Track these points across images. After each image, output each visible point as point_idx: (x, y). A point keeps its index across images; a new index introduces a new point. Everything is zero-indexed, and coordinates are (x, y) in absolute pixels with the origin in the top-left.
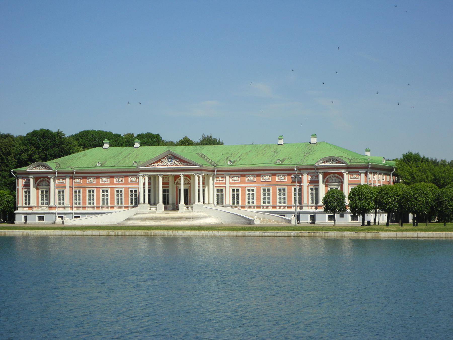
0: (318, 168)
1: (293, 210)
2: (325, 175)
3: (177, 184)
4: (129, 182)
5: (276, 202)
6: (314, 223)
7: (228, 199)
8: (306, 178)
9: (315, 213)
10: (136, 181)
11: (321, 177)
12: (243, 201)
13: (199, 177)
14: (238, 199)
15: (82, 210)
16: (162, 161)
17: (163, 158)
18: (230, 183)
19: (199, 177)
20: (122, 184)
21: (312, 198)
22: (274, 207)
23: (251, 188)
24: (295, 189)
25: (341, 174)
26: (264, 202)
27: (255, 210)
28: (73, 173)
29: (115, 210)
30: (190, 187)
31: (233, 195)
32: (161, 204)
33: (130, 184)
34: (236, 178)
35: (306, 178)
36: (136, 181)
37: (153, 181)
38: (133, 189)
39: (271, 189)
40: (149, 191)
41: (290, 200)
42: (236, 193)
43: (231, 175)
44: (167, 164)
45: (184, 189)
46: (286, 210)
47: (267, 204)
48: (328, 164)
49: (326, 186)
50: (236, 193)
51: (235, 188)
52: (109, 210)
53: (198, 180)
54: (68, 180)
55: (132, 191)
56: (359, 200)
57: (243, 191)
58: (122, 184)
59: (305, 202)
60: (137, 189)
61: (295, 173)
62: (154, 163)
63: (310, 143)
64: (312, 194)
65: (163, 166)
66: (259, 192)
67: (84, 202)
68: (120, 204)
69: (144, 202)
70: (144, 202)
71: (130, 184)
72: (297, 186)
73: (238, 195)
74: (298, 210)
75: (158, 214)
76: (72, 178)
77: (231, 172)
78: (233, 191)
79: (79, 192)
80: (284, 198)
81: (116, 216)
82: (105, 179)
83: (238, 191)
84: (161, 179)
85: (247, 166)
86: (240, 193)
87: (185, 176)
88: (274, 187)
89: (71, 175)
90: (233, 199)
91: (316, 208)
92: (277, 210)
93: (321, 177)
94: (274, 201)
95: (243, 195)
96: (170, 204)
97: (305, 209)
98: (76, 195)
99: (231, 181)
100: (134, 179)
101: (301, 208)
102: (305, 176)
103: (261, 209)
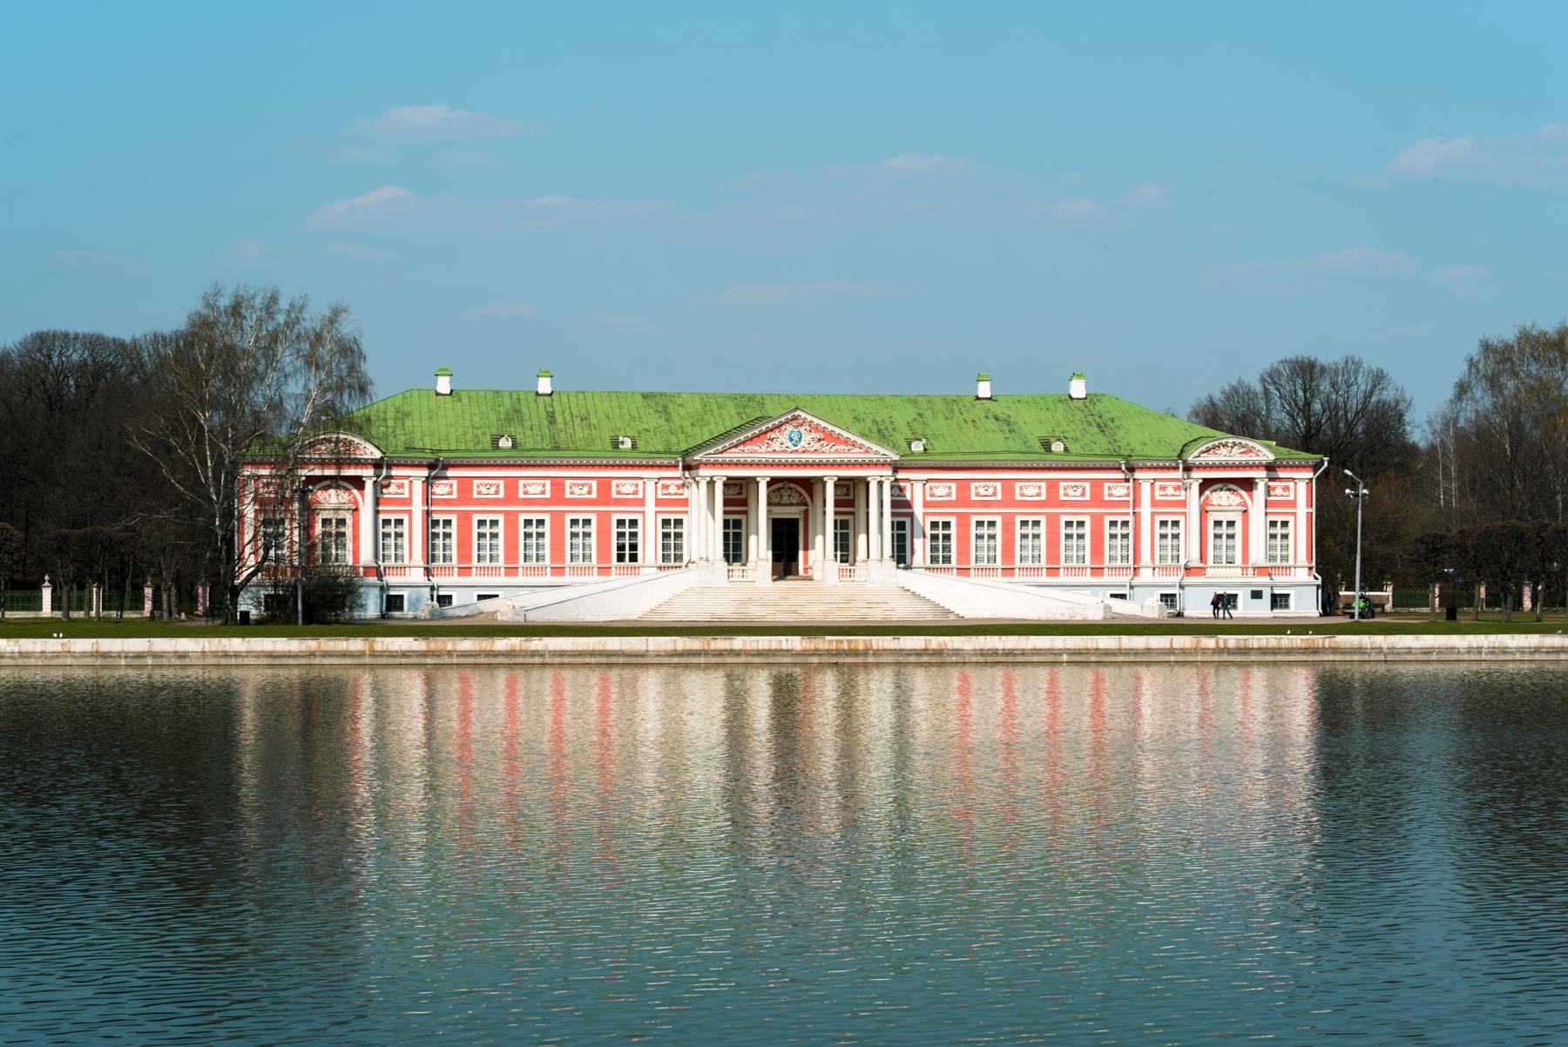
5: (1058, 558)
10: (636, 493)
12: (964, 554)
13: (880, 484)
14: (947, 548)
19: (880, 484)
30: (806, 513)
36: (636, 493)
38: (627, 517)
39: (953, 521)
48: (1222, 456)
49: (1203, 513)
51: (941, 519)
60: (639, 517)
62: (743, 443)
63: (978, 398)
73: (947, 537)
85: (953, 458)
86: (953, 531)
89: (425, 473)
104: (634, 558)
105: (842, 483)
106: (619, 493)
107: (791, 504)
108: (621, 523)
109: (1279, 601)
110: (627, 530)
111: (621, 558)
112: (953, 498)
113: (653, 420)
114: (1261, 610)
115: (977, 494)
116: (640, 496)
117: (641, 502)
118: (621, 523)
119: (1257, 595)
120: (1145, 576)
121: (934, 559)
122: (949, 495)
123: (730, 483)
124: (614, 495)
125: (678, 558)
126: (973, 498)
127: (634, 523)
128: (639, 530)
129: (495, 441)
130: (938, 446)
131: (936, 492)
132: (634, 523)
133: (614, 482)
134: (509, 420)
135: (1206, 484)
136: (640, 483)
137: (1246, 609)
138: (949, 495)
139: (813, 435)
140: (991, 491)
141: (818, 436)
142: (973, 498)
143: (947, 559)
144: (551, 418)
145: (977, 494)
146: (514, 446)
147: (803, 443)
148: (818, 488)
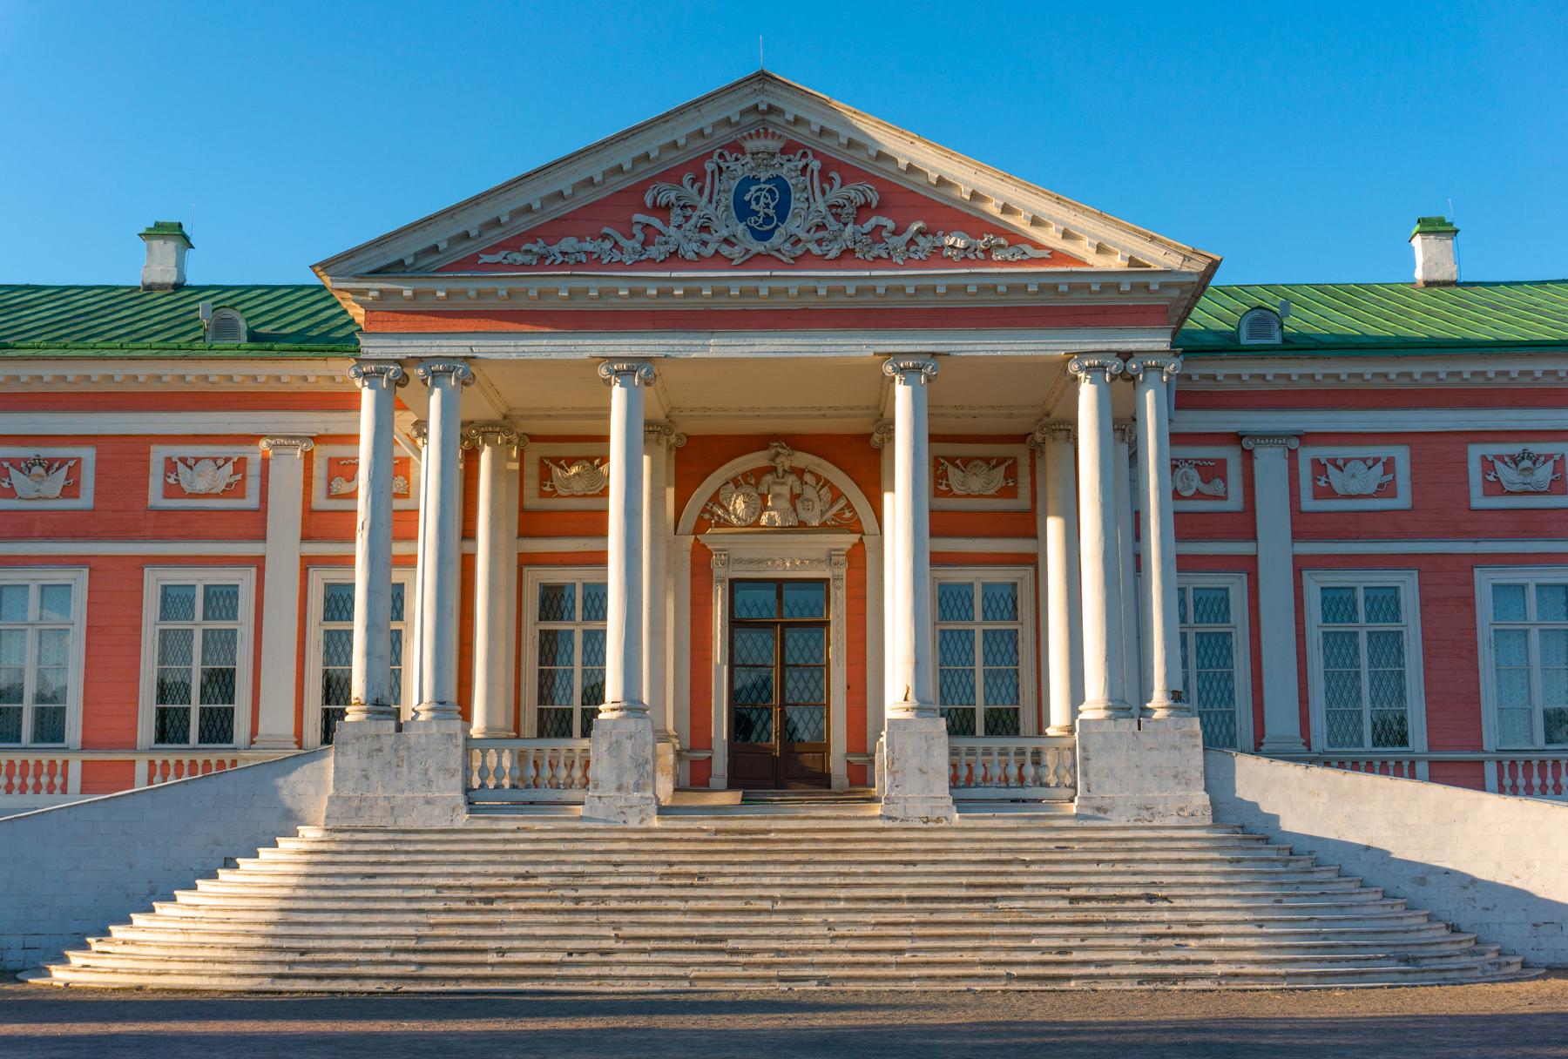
3: (700, 527)
4: (156, 498)
16: (662, 210)
17: (672, 176)
18: (1303, 526)
31: (1341, 646)
43: (1306, 438)
65: (674, 258)
78: (1337, 604)
99: (1308, 503)
104: (218, 728)
106: (173, 491)
107: (802, 527)
108: (174, 602)
110: (198, 625)
111: (169, 728)
112: (1403, 500)
115: (1494, 488)
116: (251, 501)
117: (254, 524)
118: (174, 602)
122: (1386, 490)
124: (155, 497)
126: (1478, 500)
127: (221, 601)
131: (1336, 478)
133: (158, 454)
136: (253, 454)
138: (1386, 490)
139: (837, 193)
140: (1544, 473)
141: (854, 192)
142: (1478, 500)
145: (1494, 488)
147: (793, 225)
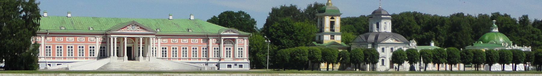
0: (221, 36)
1: (202, 61)
2: (224, 39)
6: (219, 69)
7: (160, 55)
8: (212, 41)
9: (219, 63)
11: (222, 40)
12: (170, 55)
14: (166, 54)
15: (51, 60)
18: (161, 44)
20: (83, 42)
21: (215, 54)
22: (190, 59)
23: (174, 47)
24: (203, 49)
25: (234, 40)
26: (183, 56)
27: (178, 61)
28: (46, 34)
29: (78, 60)
31: (163, 51)
32: (126, 57)
33: (89, 42)
34: (164, 40)
35: (212, 41)
37: (120, 41)
40: (117, 48)
41: (200, 55)
42: (164, 50)
44: (130, 30)
45: (127, 47)
46: (198, 61)
47: (185, 57)
48: (228, 33)
50: (164, 50)
51: (164, 47)
52: (73, 60)
53: (153, 41)
54: (43, 38)
55: (91, 47)
56: (303, 55)
57: (169, 49)
58: (83, 42)
59: (211, 57)
61: (206, 38)
64: (215, 52)
66: (180, 49)
67: (54, 54)
68: (81, 56)
69: (114, 55)
70: (114, 55)
71: (89, 42)
72: (205, 46)
73: (166, 51)
74: (205, 61)
75: (124, 63)
76: (46, 38)
77: (163, 36)
78: (163, 48)
79: (50, 47)
80: (196, 54)
81: (97, 64)
82: (71, 38)
83: (166, 48)
84: (126, 39)
86: (167, 50)
87: (128, 37)
88: (190, 47)
90: (163, 54)
91: (220, 60)
92: (192, 61)
93: (222, 40)
94: (190, 55)
95: (169, 51)
96: (131, 57)
97: (211, 61)
98: (47, 50)
100: (92, 39)
101: (208, 60)
102: (211, 40)
103: (182, 60)
105: (144, 39)
109: (241, 66)
113: (96, 23)
114: (237, 68)
119: (236, 65)
120: (211, 61)
121: (163, 56)
123: (118, 38)
125: (104, 55)
127: (93, 47)
128: (95, 49)
129: (60, 28)
130: (162, 30)
132: (93, 47)
134: (62, 23)
135: (224, 39)
137: (233, 68)
143: (166, 56)
144: (72, 23)
146: (65, 29)
148: (137, 40)
